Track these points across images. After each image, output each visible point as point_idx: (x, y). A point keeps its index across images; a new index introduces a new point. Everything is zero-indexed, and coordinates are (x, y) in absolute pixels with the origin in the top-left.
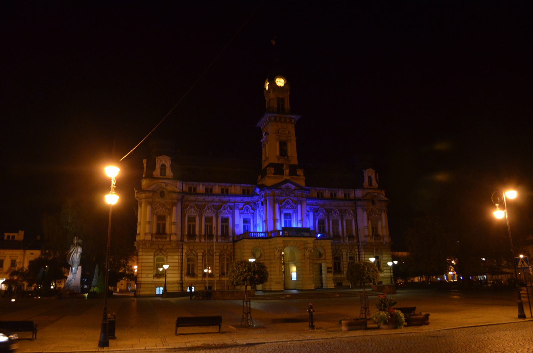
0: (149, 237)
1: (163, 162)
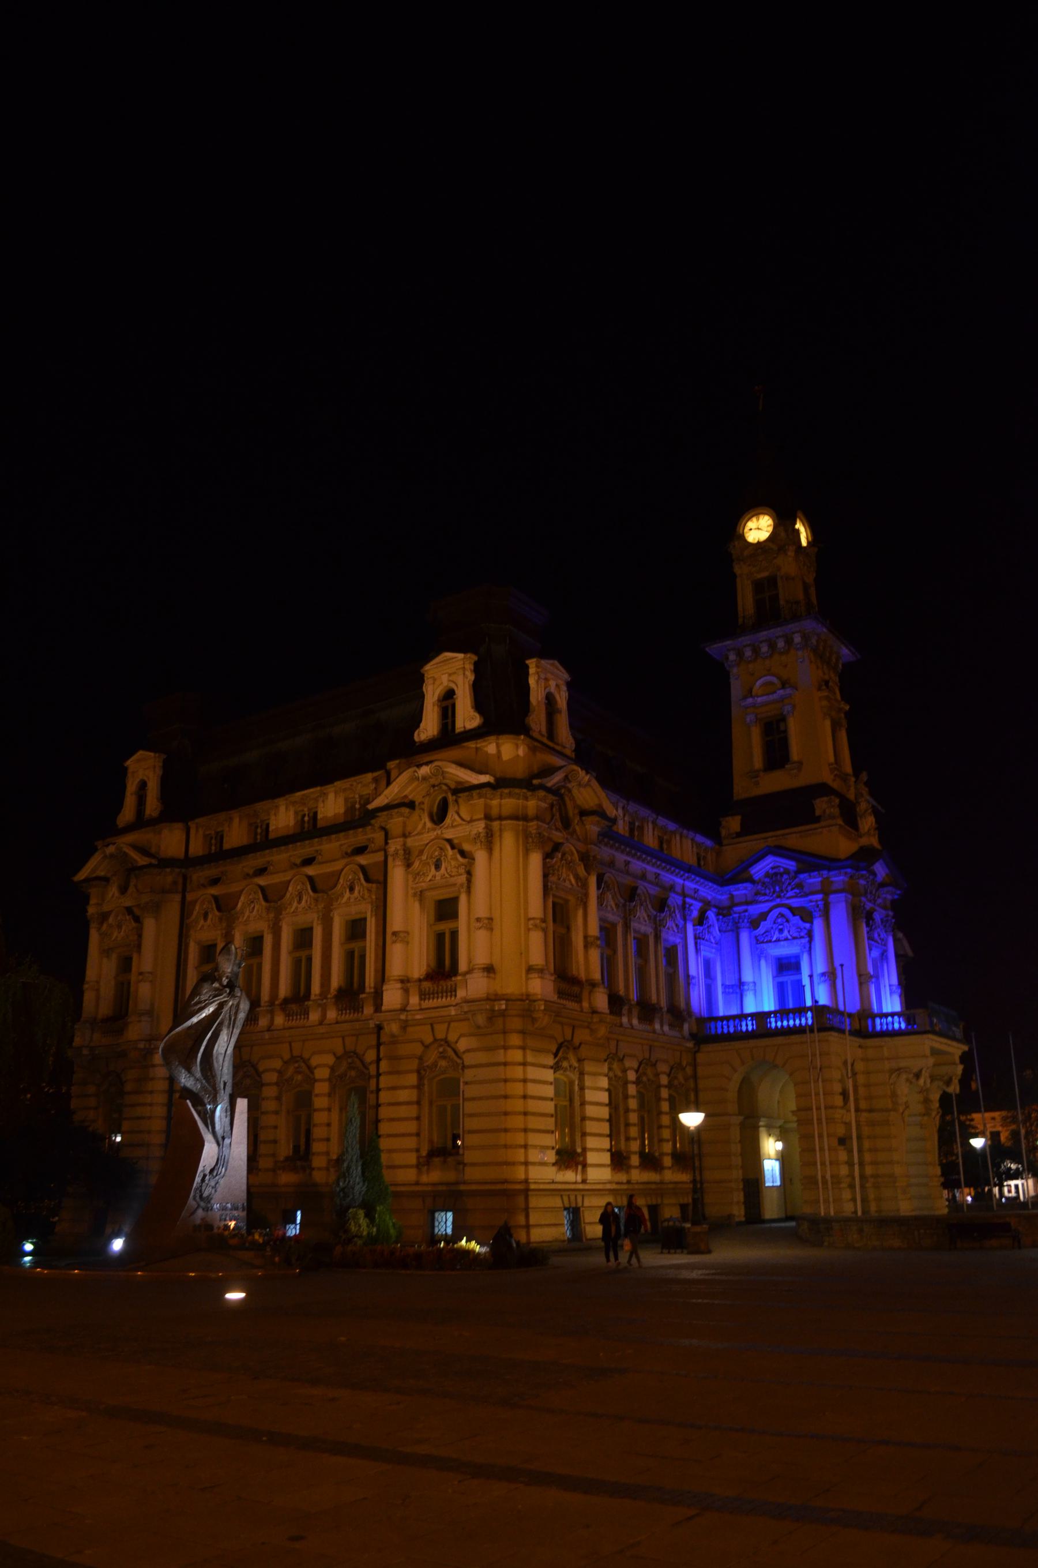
1: (553, 689)
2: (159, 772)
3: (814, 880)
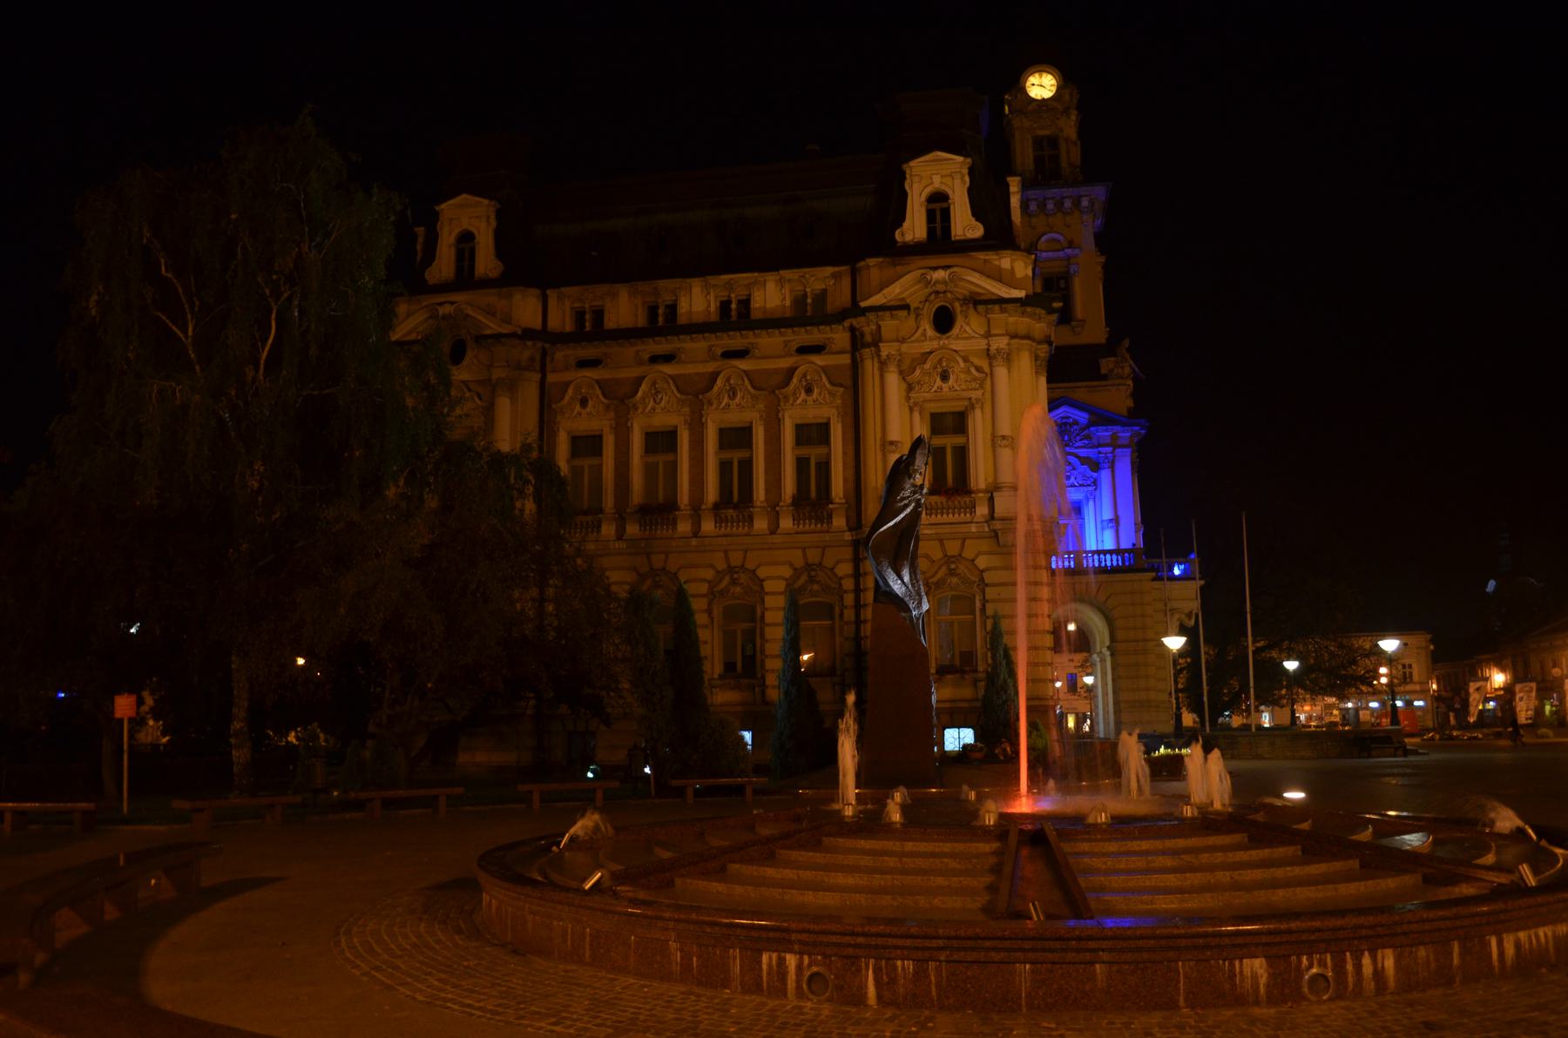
2: (494, 223)
3: (1104, 433)
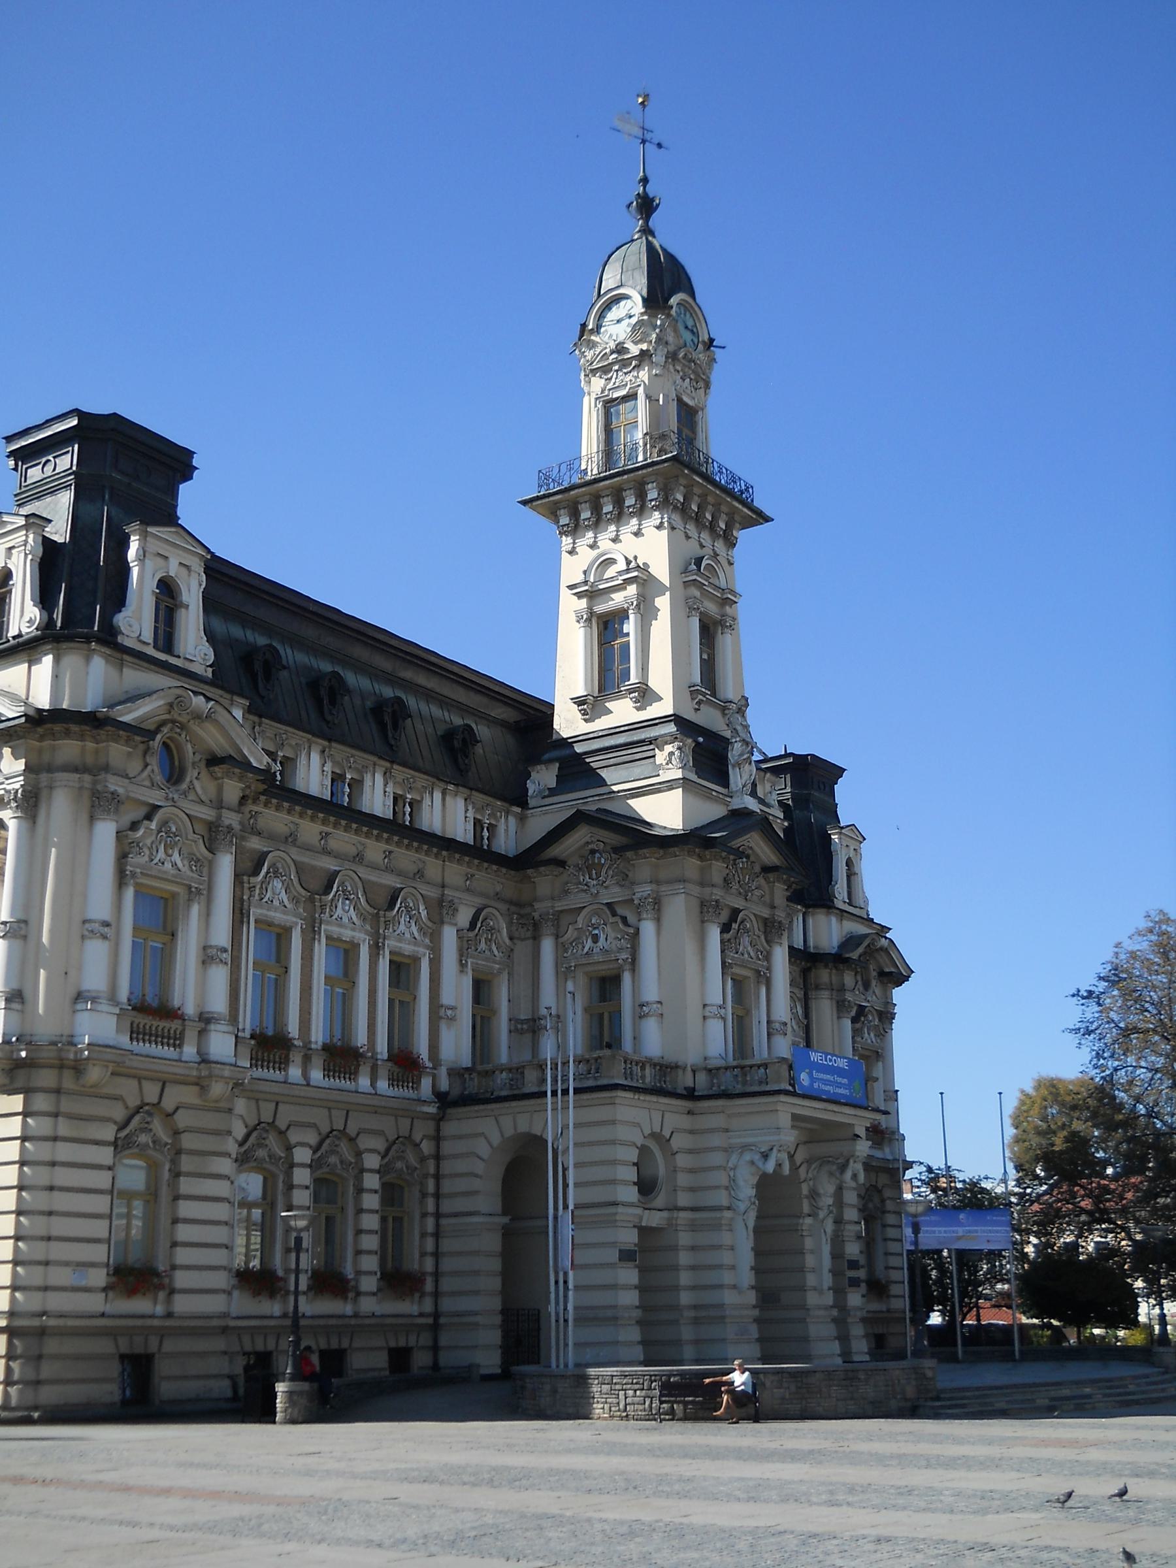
0: (97, 1027)
1: (173, 570)
